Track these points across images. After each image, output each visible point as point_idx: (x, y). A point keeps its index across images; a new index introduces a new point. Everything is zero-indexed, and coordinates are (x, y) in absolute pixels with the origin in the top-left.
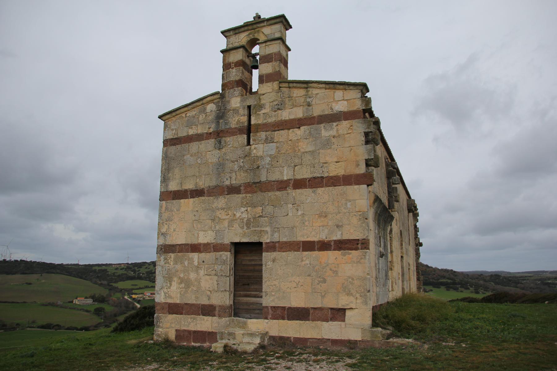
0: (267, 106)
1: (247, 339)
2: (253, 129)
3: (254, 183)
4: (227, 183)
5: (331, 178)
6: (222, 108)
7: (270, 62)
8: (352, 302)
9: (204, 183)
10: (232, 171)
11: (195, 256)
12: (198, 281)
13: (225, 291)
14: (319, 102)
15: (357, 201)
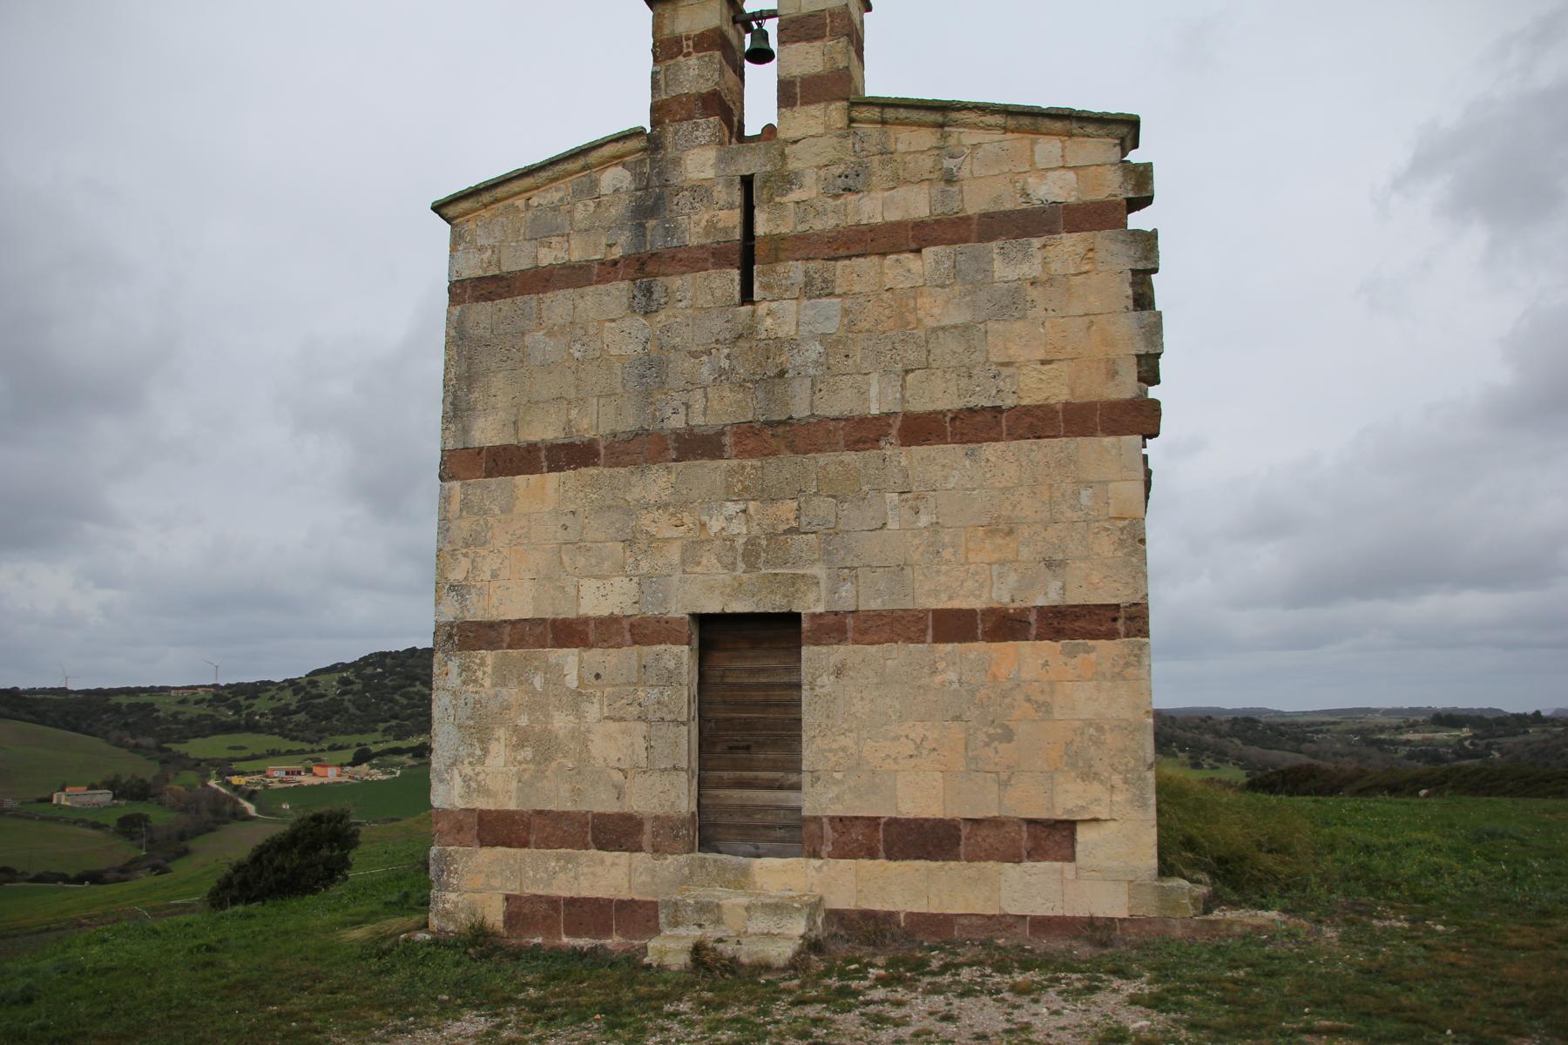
0: (809, 179)
1: (760, 924)
2: (760, 251)
3: (769, 424)
4: (677, 422)
5: (1028, 410)
6: (655, 181)
7: (816, 39)
8: (1097, 800)
9: (591, 423)
10: (691, 385)
11: (569, 660)
12: (582, 738)
13: (675, 768)
14: (984, 172)
15: (1111, 486)
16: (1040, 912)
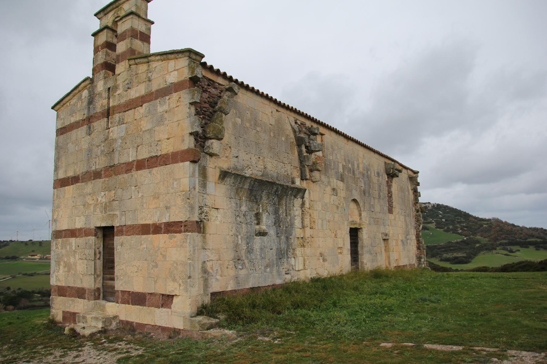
0: (121, 87)
3: (111, 167)
4: (93, 168)
11: (73, 240)
12: (75, 264)
16: (164, 325)
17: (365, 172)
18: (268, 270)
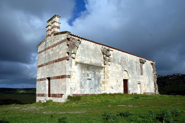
11: (41, 82)
17: (130, 62)
18: (91, 90)
